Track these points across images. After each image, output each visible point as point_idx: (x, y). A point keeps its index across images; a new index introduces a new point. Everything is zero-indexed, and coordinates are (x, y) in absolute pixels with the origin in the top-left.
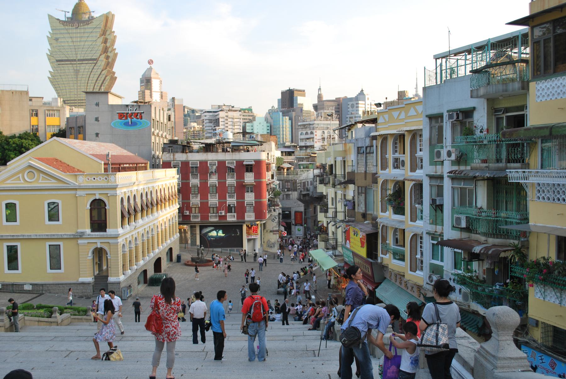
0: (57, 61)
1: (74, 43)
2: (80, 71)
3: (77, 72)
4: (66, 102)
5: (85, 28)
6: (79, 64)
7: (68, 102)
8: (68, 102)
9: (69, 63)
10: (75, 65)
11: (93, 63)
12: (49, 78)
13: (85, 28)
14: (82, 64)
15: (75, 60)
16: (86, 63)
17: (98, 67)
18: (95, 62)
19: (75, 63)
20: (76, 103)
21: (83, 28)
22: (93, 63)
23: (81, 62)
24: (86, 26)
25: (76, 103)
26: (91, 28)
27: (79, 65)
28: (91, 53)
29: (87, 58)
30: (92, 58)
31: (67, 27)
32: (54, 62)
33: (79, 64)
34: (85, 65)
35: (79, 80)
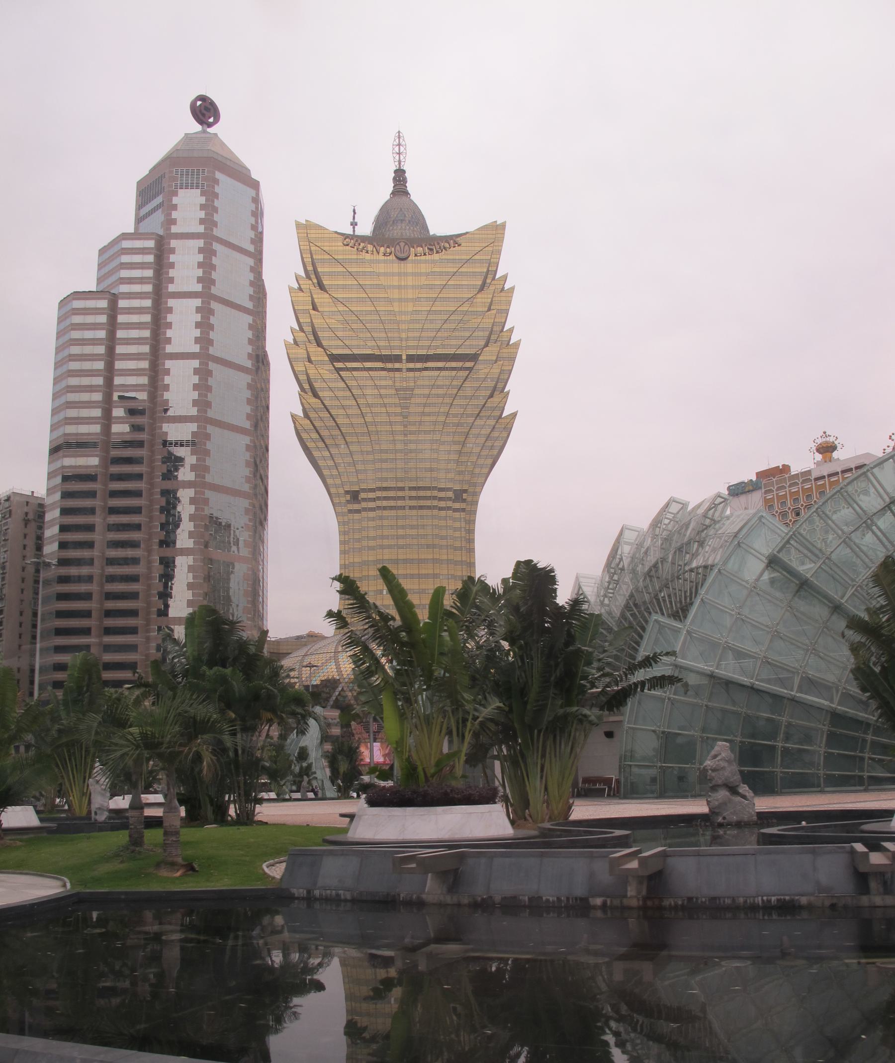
0: (334, 358)
1: (396, 304)
2: (417, 391)
3: (405, 394)
4: (363, 495)
5: (434, 262)
6: (410, 370)
7: (371, 495)
8: (371, 495)
9: (379, 365)
10: (397, 374)
11: (461, 369)
12: (294, 417)
13: (434, 262)
14: (426, 369)
15: (398, 358)
16: (439, 369)
17: (476, 384)
18: (469, 364)
19: (397, 365)
20: (403, 498)
21: (426, 262)
22: (461, 369)
23: (419, 365)
24: (436, 257)
25: (403, 498)
26: (454, 261)
27: (411, 374)
28: (456, 338)
29: (439, 351)
30: (459, 352)
31: (368, 257)
32: (322, 362)
33: (410, 370)
34: (436, 373)
35: (414, 423)
